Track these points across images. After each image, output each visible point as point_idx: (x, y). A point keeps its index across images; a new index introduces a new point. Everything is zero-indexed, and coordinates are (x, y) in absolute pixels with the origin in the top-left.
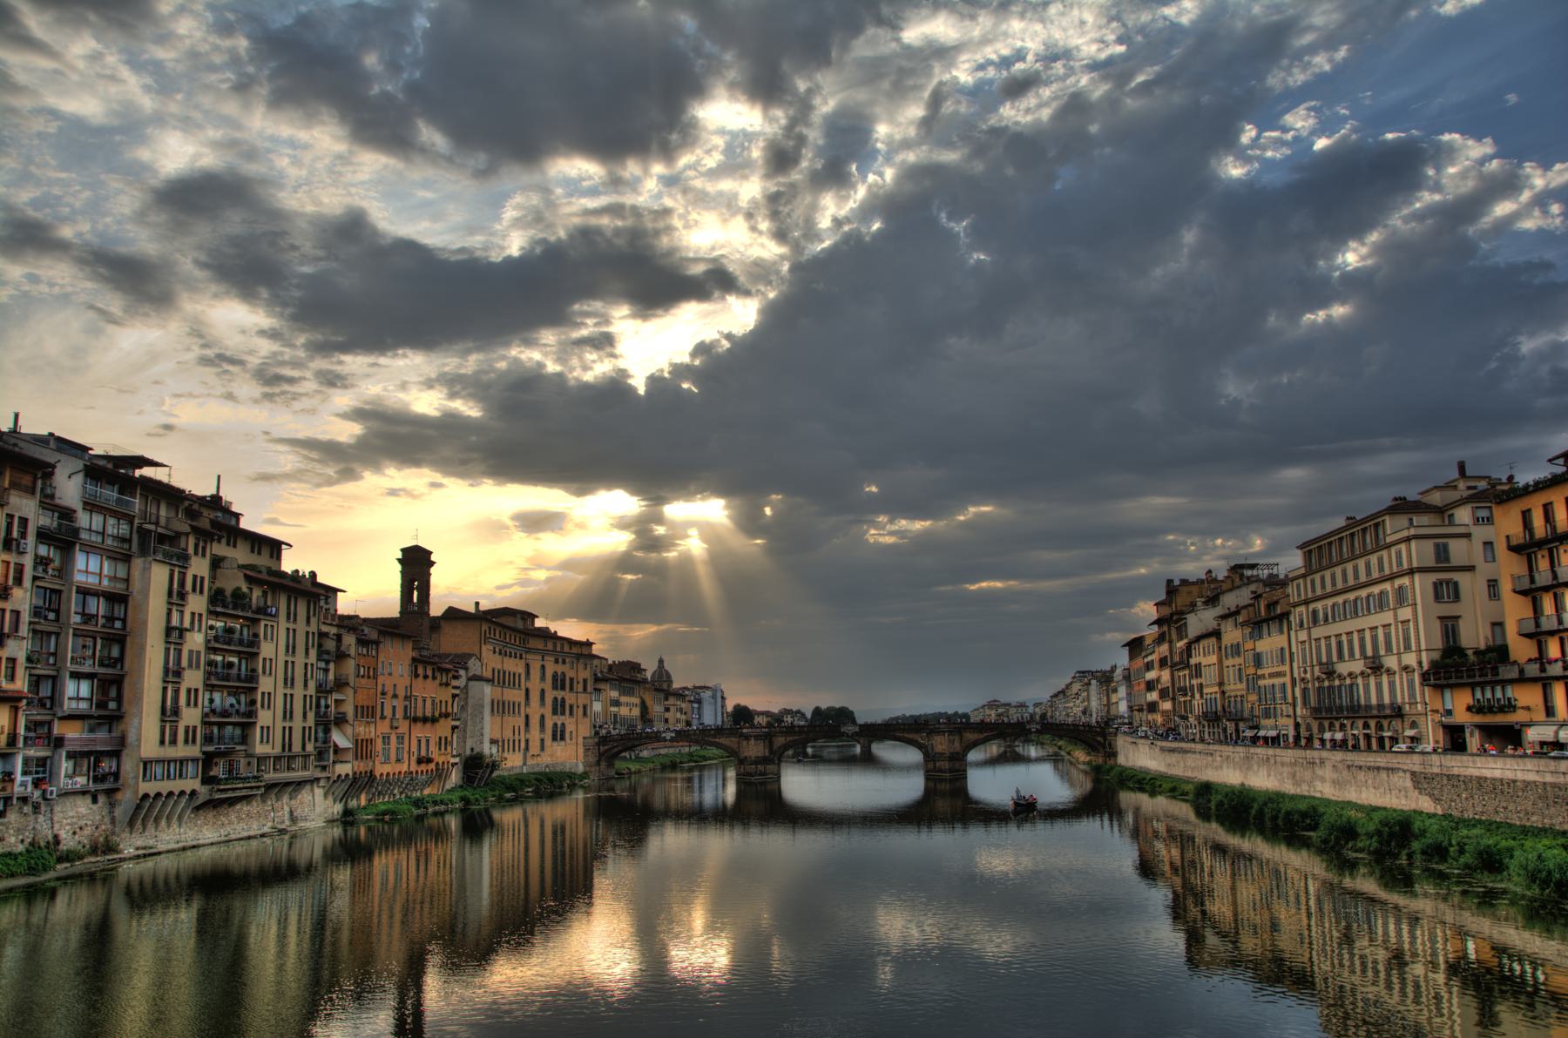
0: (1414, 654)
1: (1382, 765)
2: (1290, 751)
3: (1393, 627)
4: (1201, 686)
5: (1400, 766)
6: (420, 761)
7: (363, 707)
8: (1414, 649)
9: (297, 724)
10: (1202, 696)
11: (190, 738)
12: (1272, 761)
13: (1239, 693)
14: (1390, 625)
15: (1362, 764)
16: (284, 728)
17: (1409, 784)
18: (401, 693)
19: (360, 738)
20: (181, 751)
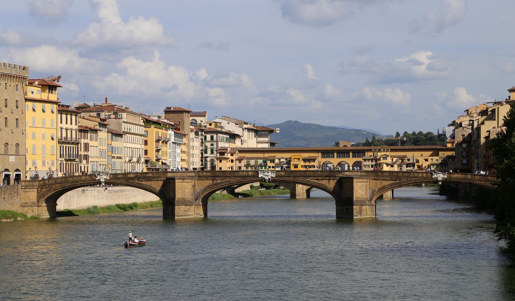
4: (86, 157)
10: (88, 162)
13: (104, 163)
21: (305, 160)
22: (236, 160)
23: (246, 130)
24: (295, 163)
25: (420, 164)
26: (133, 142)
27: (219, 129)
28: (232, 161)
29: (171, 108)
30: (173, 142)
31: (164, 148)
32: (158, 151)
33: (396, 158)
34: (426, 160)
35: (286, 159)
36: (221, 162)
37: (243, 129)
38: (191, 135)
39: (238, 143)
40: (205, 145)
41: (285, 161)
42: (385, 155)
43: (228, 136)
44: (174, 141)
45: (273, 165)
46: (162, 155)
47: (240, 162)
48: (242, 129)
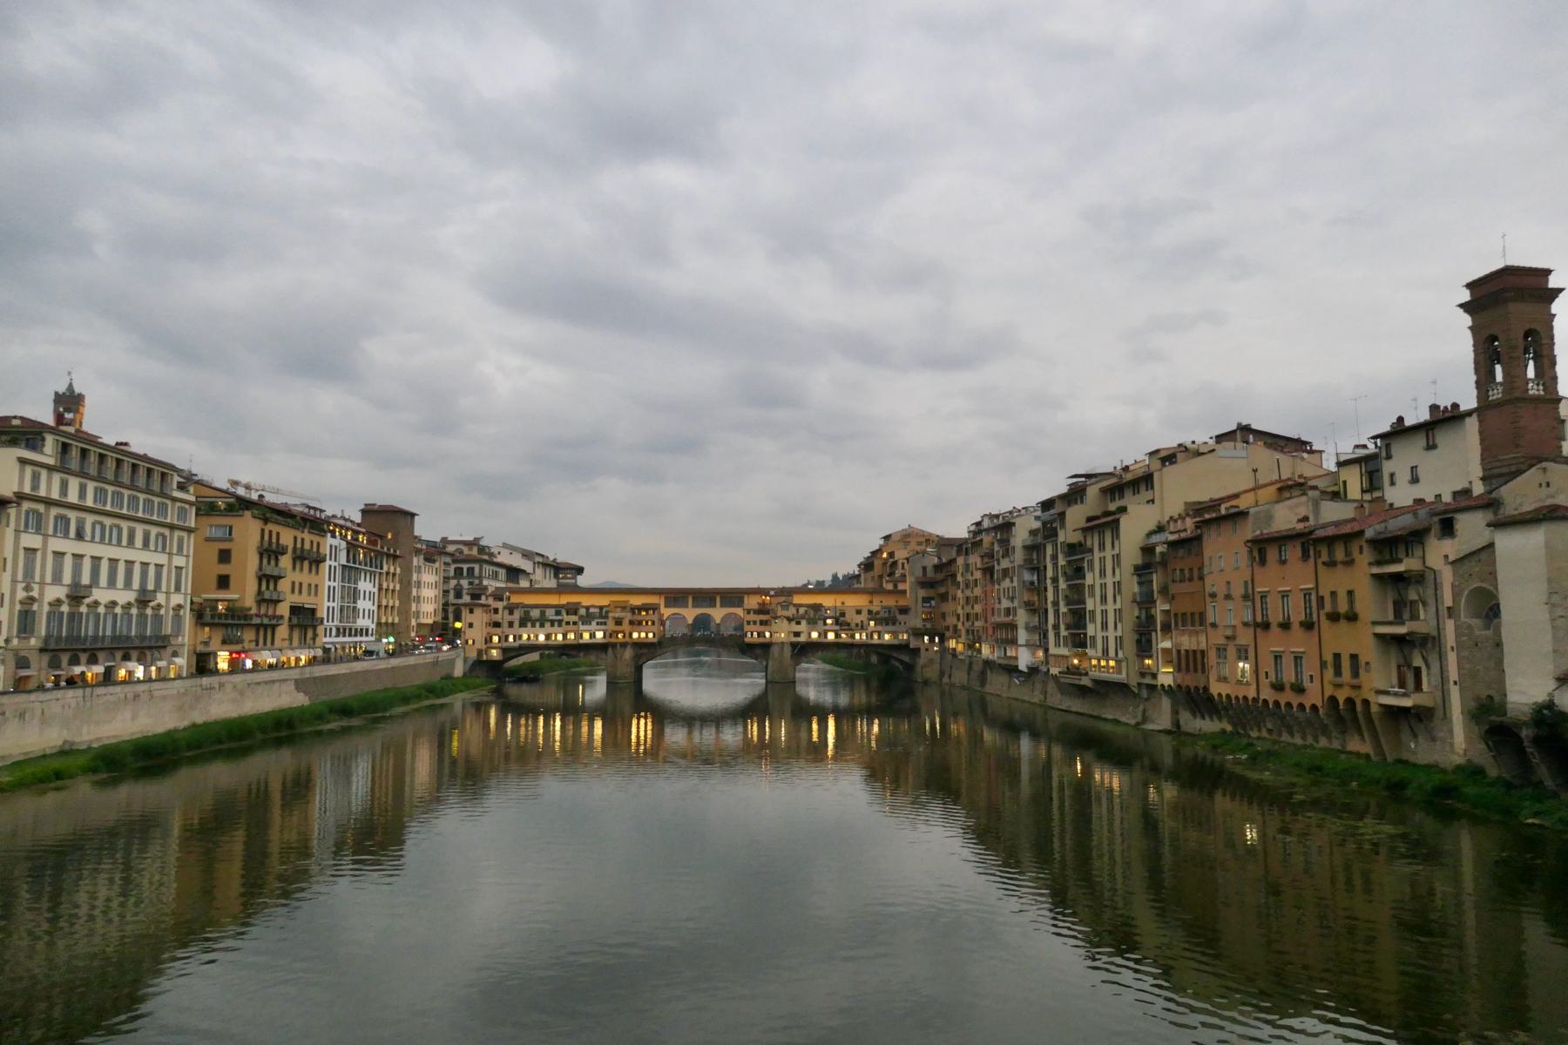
0: (182, 596)
1: (276, 678)
2: (62, 692)
3: (165, 570)
5: (287, 677)
6: (1278, 687)
7: (1184, 614)
8: (183, 591)
9: (1111, 634)
11: (1066, 645)
12: (145, 697)
14: (162, 566)
15: (258, 681)
16: (1103, 637)
17: (292, 687)
18: (1238, 591)
19: (1183, 649)
20: (1064, 651)
21: (633, 610)
22: (505, 608)
23: (541, 566)
24: (617, 615)
25: (848, 618)
26: (107, 541)
27: (486, 557)
28: (496, 611)
29: (374, 505)
30: (343, 566)
31: (290, 573)
32: (268, 579)
33: (805, 608)
34: (859, 612)
35: (601, 608)
36: (471, 611)
37: (534, 563)
38: (415, 560)
39: (524, 584)
40: (459, 582)
41: (597, 610)
42: (785, 602)
43: (502, 573)
44: (344, 562)
45: (573, 618)
46: (293, 591)
47: (511, 613)
48: (532, 563)
